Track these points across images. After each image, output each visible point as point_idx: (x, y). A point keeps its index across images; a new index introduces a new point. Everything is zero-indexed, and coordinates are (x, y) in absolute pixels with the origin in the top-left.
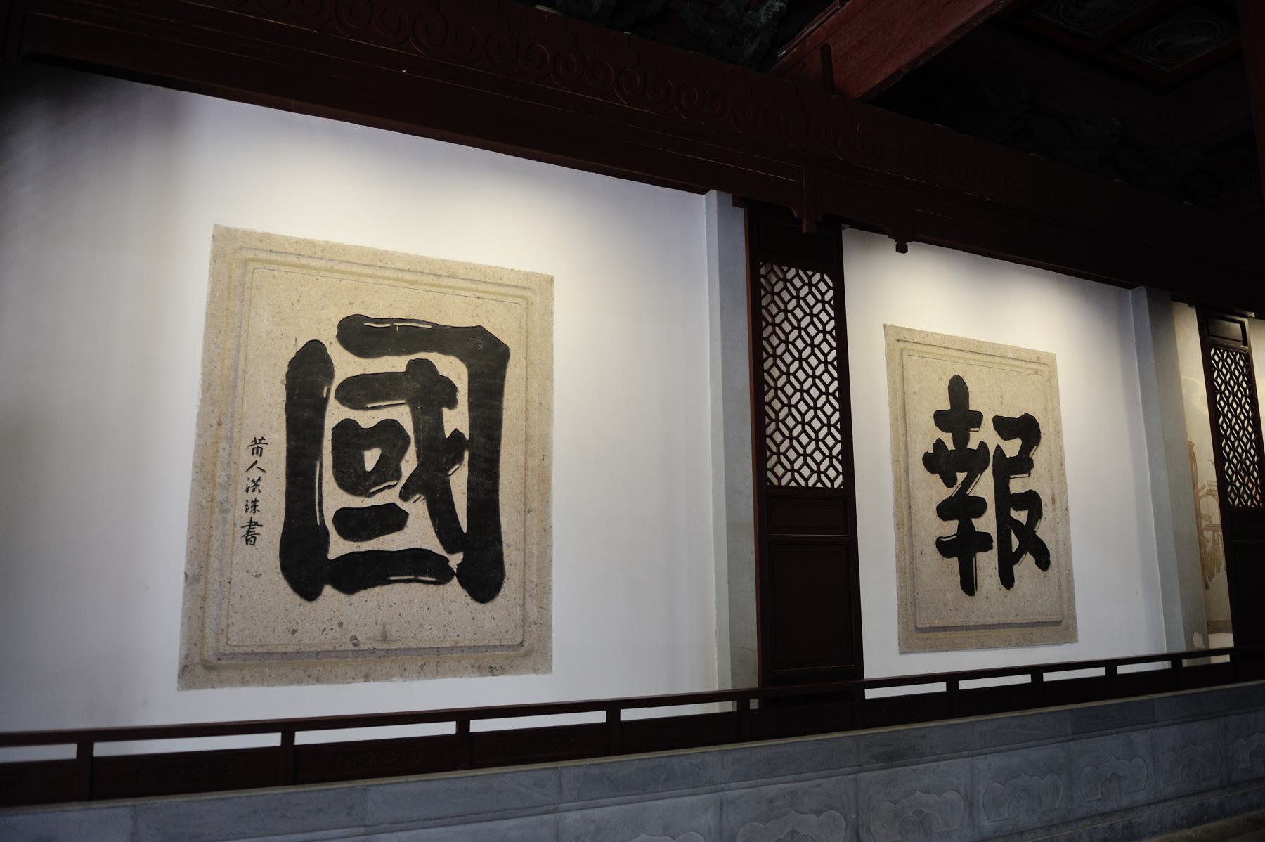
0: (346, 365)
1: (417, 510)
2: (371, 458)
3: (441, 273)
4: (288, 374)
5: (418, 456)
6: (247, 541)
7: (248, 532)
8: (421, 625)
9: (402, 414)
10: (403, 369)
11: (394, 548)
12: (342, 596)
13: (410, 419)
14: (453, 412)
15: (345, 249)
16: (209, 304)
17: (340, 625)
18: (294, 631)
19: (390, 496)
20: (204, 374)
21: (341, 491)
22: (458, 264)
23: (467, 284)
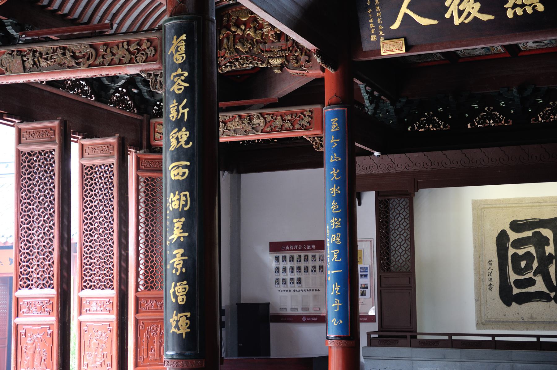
0: (513, 236)
1: (539, 279)
2: (523, 264)
3: (541, 201)
4: (496, 241)
5: (538, 262)
6: (490, 290)
7: (490, 287)
8: (543, 314)
9: (532, 249)
10: (531, 235)
11: (532, 291)
12: (518, 305)
13: (534, 251)
14: (549, 247)
15: (509, 199)
16: (473, 223)
17: (518, 314)
18: (505, 315)
19: (530, 275)
20: (474, 244)
21: (515, 274)
22: (547, 197)
23: (551, 204)
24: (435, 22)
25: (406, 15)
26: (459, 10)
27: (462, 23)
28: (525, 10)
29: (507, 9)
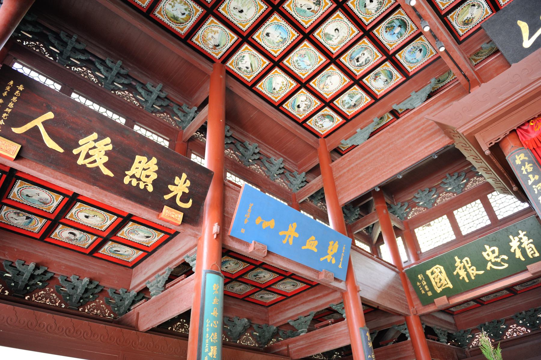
24: (61, 150)
25: (36, 128)
26: (88, 153)
27: (84, 165)
28: (138, 184)
29: (127, 175)
